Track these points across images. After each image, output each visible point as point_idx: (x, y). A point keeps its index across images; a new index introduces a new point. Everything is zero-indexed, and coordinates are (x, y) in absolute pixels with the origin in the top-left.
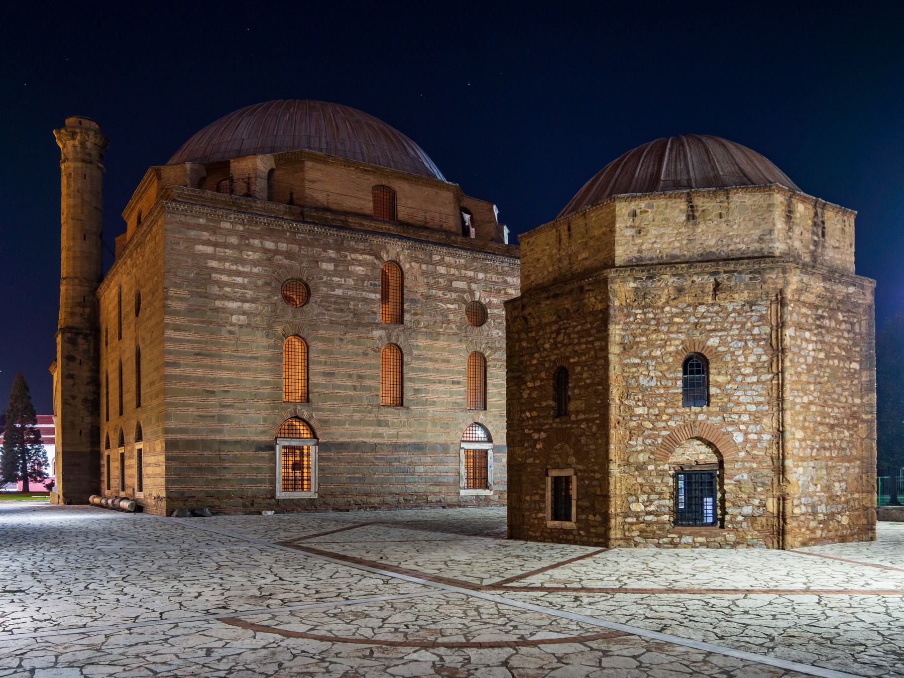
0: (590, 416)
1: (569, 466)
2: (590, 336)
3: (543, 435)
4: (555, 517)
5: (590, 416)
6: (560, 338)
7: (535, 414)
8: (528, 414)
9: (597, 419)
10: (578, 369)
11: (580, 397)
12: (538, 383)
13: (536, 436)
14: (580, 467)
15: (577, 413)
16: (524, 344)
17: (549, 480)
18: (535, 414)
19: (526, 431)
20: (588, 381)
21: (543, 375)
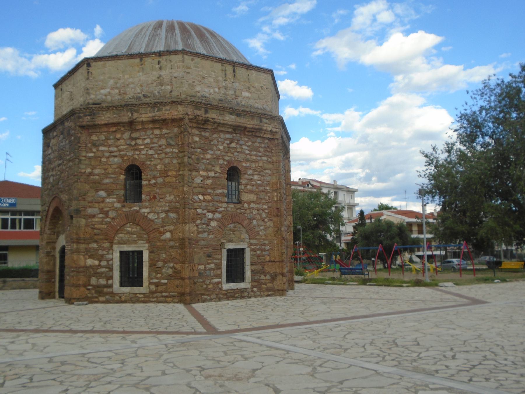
0: (260, 206)
1: (243, 241)
2: (259, 152)
3: (217, 215)
4: (230, 279)
5: (260, 206)
6: (233, 145)
7: (208, 197)
8: (201, 197)
9: (265, 209)
10: (250, 172)
11: (252, 192)
12: (212, 174)
13: (210, 215)
14: (253, 241)
15: (249, 203)
16: (197, 139)
17: (224, 252)
18: (208, 197)
19: (199, 211)
20: (259, 182)
21: (218, 169)
